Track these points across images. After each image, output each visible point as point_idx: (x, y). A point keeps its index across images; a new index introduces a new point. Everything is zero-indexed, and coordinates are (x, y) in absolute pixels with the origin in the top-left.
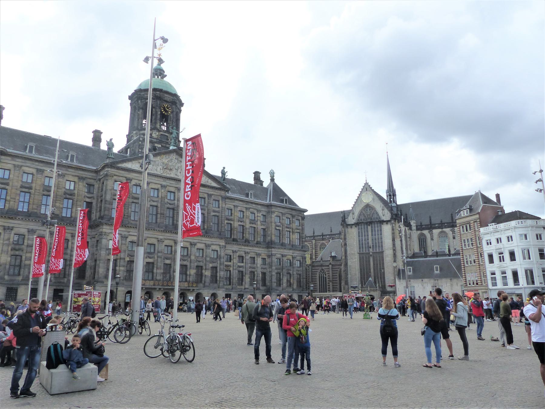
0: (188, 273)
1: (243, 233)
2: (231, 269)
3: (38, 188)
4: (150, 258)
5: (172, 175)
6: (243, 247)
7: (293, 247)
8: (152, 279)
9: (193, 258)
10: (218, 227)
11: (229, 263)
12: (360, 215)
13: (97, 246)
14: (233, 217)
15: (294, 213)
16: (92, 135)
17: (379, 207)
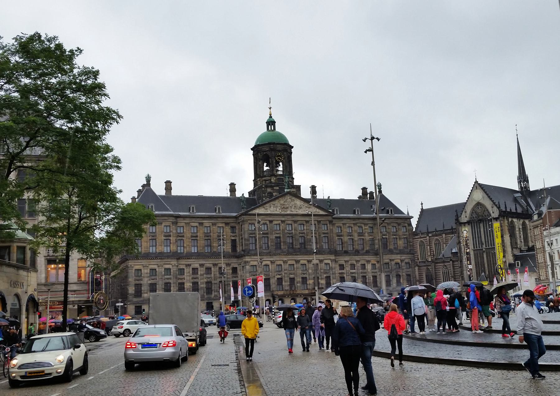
0: (308, 283)
1: (353, 245)
2: (345, 276)
3: (201, 236)
4: (279, 275)
5: (288, 212)
6: (354, 257)
7: (401, 252)
8: (283, 290)
9: (310, 271)
10: (328, 245)
11: (343, 271)
12: (473, 213)
13: (243, 270)
14: (342, 233)
15: (399, 221)
16: (229, 187)
17: (488, 204)
